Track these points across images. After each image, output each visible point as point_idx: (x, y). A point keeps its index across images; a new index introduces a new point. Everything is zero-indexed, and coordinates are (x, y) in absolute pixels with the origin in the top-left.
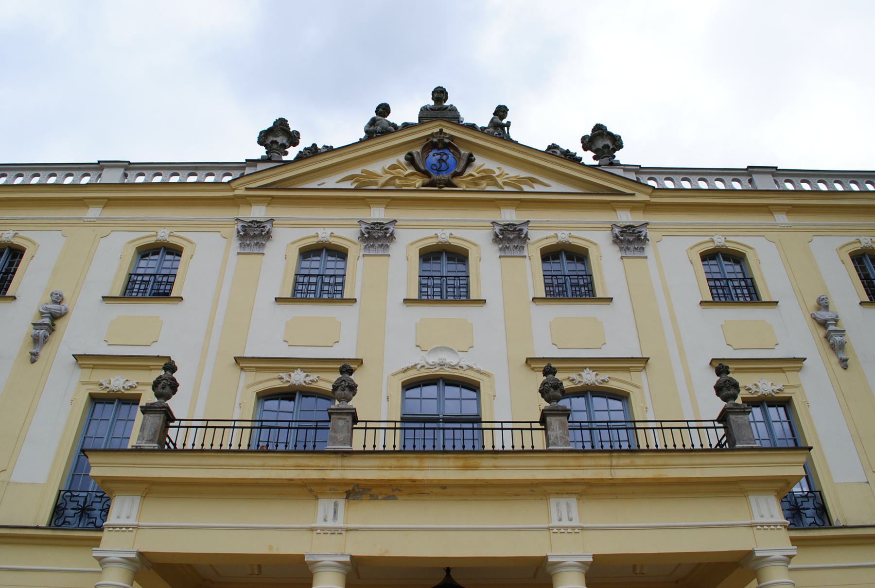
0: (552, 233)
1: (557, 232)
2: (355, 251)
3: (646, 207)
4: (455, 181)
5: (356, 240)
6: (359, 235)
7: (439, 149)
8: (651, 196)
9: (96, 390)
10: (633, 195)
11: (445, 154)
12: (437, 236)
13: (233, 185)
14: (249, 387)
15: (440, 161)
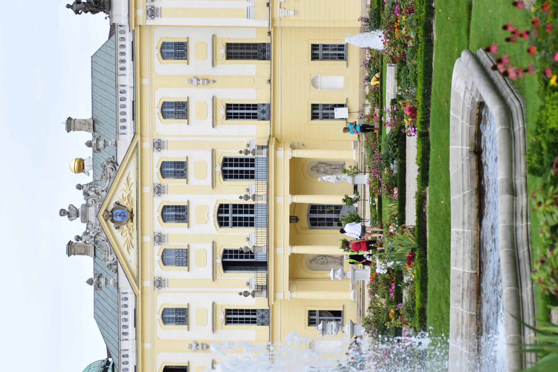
0: (155, 175)
1: (155, 172)
2: (166, 246)
3: (141, 136)
4: (130, 210)
5: (159, 246)
6: (159, 245)
7: (114, 216)
8: (138, 135)
9: (224, 323)
10: (138, 141)
11: (116, 214)
12: (158, 217)
13: (137, 294)
14: (222, 276)
15: (120, 215)
